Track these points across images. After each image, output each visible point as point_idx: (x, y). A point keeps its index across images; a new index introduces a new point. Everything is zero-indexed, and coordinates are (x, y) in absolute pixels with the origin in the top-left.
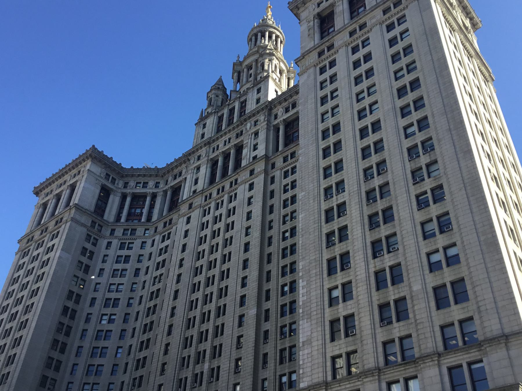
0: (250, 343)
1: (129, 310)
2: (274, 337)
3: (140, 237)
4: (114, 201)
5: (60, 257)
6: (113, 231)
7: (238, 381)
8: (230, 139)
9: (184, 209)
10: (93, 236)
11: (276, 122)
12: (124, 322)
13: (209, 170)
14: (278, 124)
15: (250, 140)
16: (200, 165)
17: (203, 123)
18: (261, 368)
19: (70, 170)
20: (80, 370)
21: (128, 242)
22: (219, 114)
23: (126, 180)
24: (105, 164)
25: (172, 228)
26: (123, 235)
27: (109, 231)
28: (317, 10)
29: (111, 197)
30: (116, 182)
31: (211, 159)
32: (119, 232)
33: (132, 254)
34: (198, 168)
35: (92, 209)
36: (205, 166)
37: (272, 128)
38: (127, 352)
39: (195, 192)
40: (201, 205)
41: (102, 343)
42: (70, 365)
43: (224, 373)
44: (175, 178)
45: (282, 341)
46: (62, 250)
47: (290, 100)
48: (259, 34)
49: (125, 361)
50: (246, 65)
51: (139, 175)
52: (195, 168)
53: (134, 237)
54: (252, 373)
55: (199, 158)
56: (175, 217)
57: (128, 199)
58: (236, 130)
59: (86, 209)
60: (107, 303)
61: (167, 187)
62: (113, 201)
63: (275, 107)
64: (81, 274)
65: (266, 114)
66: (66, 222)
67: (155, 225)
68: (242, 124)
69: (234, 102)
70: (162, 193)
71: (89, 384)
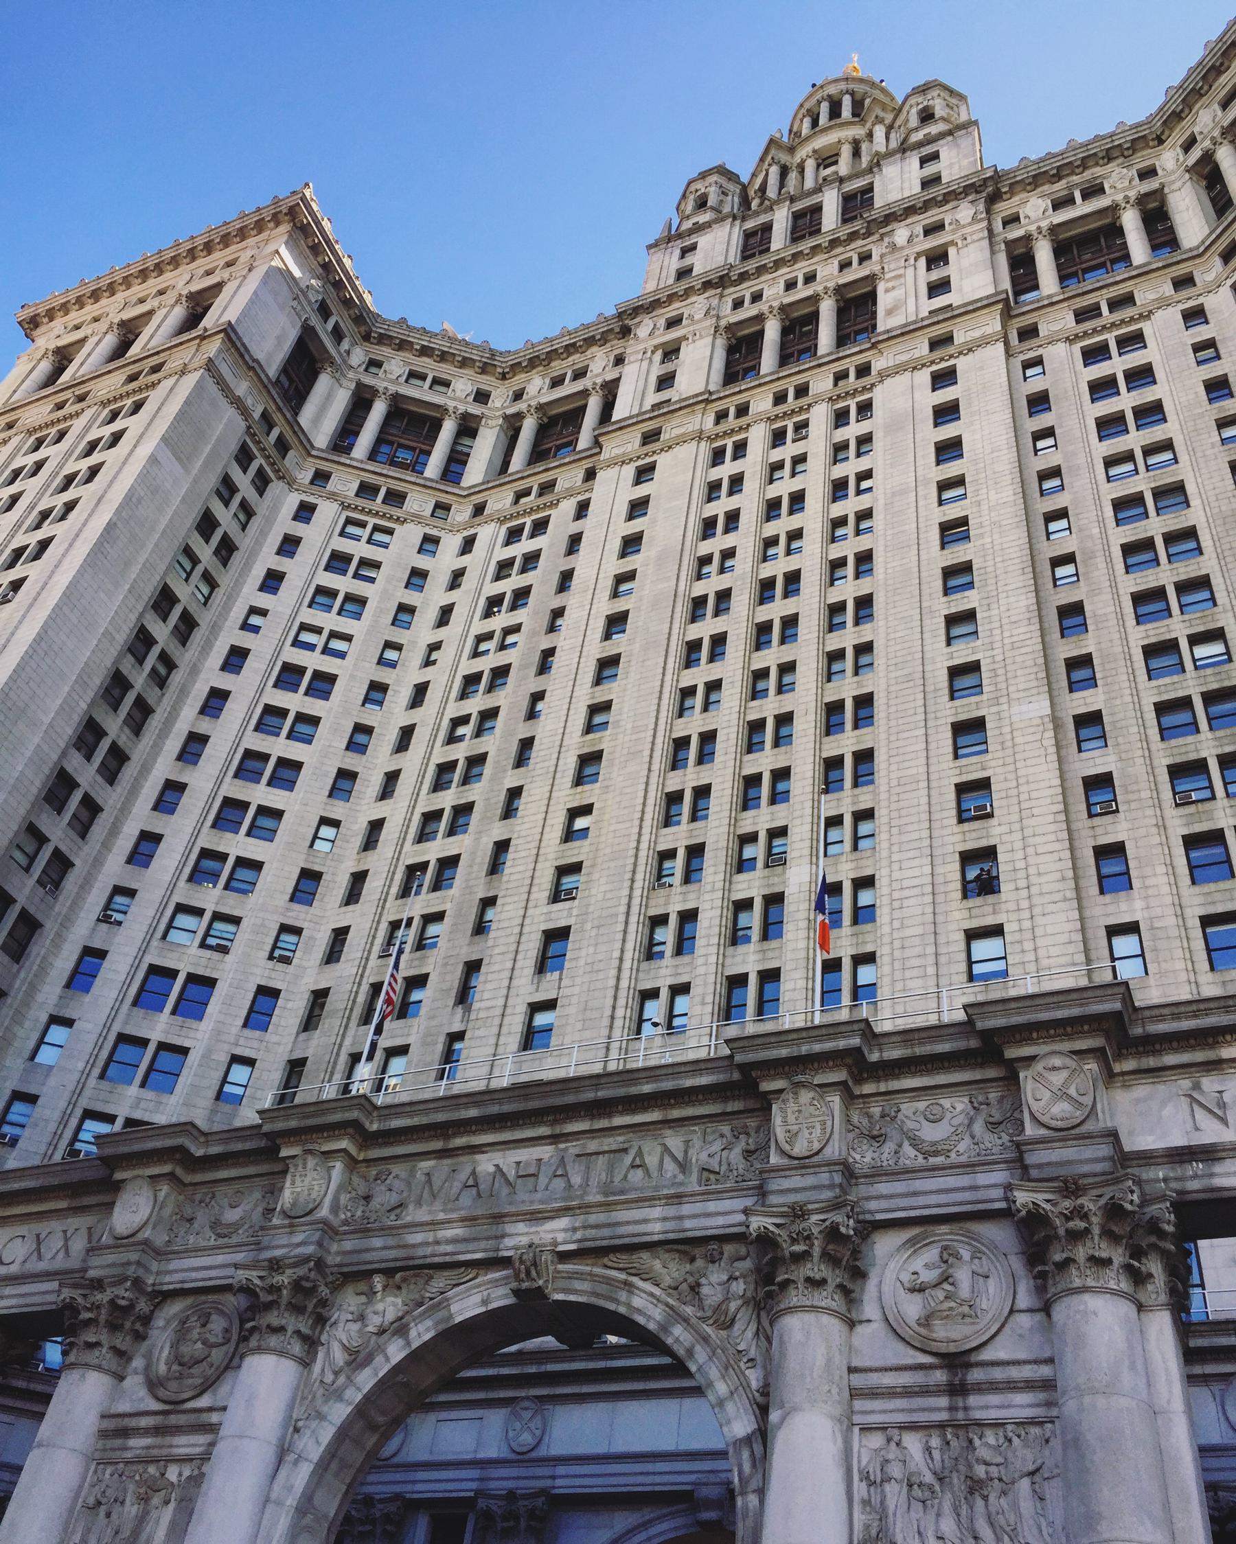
0: (1033, 803)
1: (371, 716)
2: (1146, 794)
3: (417, 518)
5: (153, 460)
6: (321, 477)
7: (990, 921)
8: (810, 278)
9: (625, 444)
10: (259, 461)
11: (1016, 233)
14: (1028, 238)
15: (910, 271)
16: (685, 338)
17: (679, 244)
18: (1096, 890)
19: (192, 255)
20: (170, 859)
21: (372, 521)
22: (750, 224)
23: (383, 352)
25: (554, 505)
29: (323, 382)
31: (729, 328)
32: (345, 483)
34: (671, 352)
35: (273, 370)
36: (710, 339)
37: (1003, 246)
38: (358, 840)
40: (701, 432)
43: (906, 893)
44: (557, 382)
45: (1191, 809)
46: (165, 439)
47: (1075, 179)
48: (847, 102)
49: (350, 865)
50: (815, 151)
52: (656, 348)
53: (396, 512)
54: (1071, 894)
55: (673, 323)
56: (569, 477)
57: (379, 410)
58: (839, 250)
59: (255, 360)
60: (289, 676)
61: (521, 406)
62: (329, 398)
63: (1012, 192)
64: (206, 552)
65: (981, 207)
66: (183, 373)
67: (477, 499)
68: (869, 234)
69: (818, 190)
70: (500, 421)
71: (199, 912)
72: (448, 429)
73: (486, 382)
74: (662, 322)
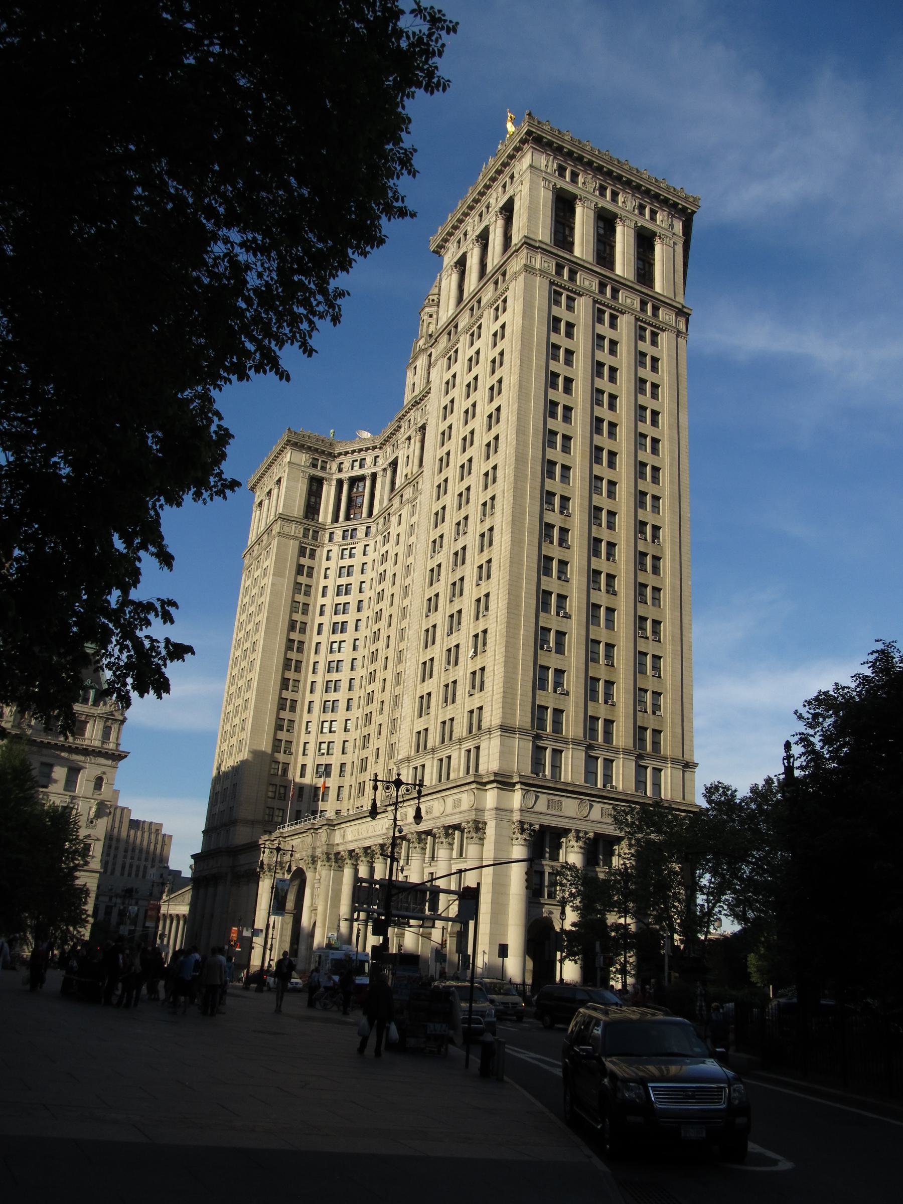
4: (328, 492)
5: (273, 584)
6: (332, 533)
12: (354, 650)
13: (418, 445)
20: (317, 707)
24: (310, 448)
26: (343, 539)
27: (327, 536)
28: (455, 260)
29: (325, 487)
30: (328, 467)
33: (357, 561)
39: (406, 476)
41: (334, 676)
42: (307, 703)
51: (354, 451)
53: (354, 540)
72: (368, 483)
73: (377, 452)
74: (407, 423)
